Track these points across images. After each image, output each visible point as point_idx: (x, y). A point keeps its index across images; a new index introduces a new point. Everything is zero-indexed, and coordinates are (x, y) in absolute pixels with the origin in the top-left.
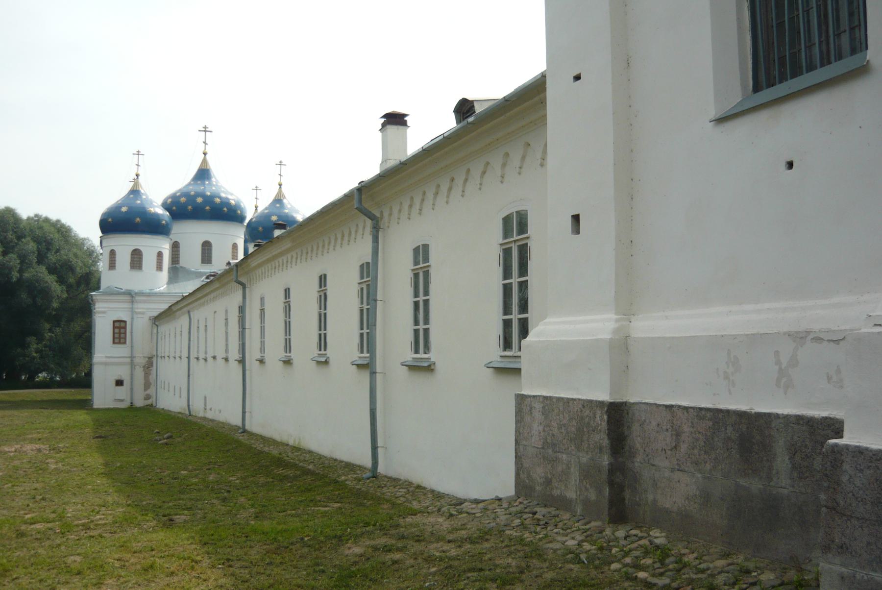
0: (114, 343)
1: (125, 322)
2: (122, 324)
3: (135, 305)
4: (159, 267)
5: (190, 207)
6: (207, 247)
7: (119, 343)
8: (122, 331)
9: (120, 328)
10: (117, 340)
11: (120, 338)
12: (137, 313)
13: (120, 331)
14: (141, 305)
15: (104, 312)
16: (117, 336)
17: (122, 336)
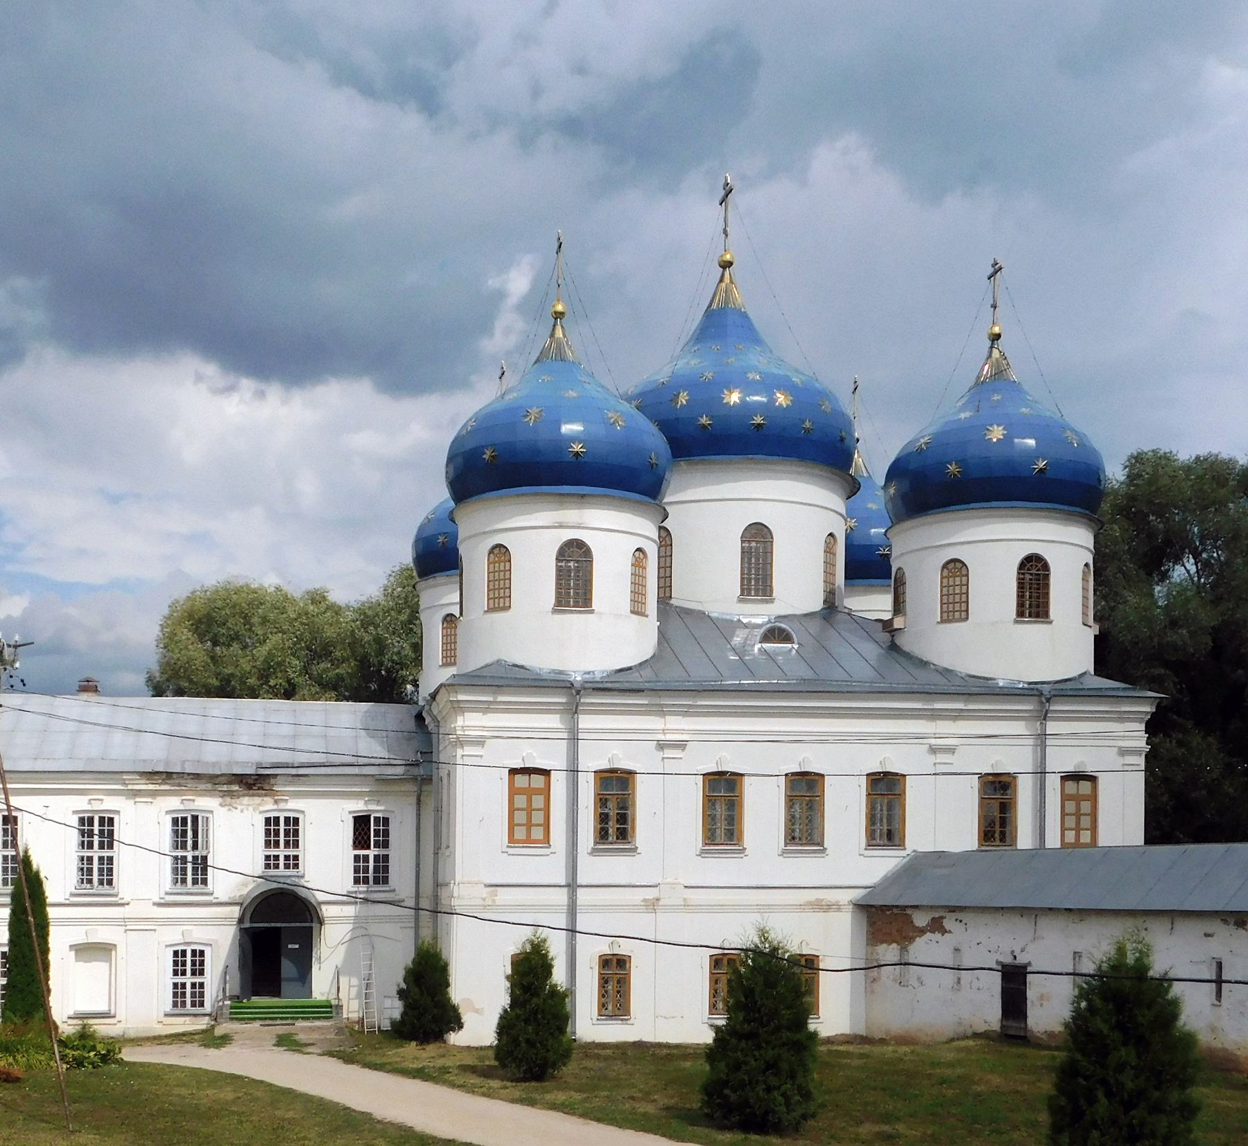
0: (512, 839)
1: (546, 773)
7: (528, 841)
8: (538, 801)
9: (530, 792)
10: (520, 833)
11: (529, 825)
13: (529, 801)
15: (480, 742)
16: (520, 817)
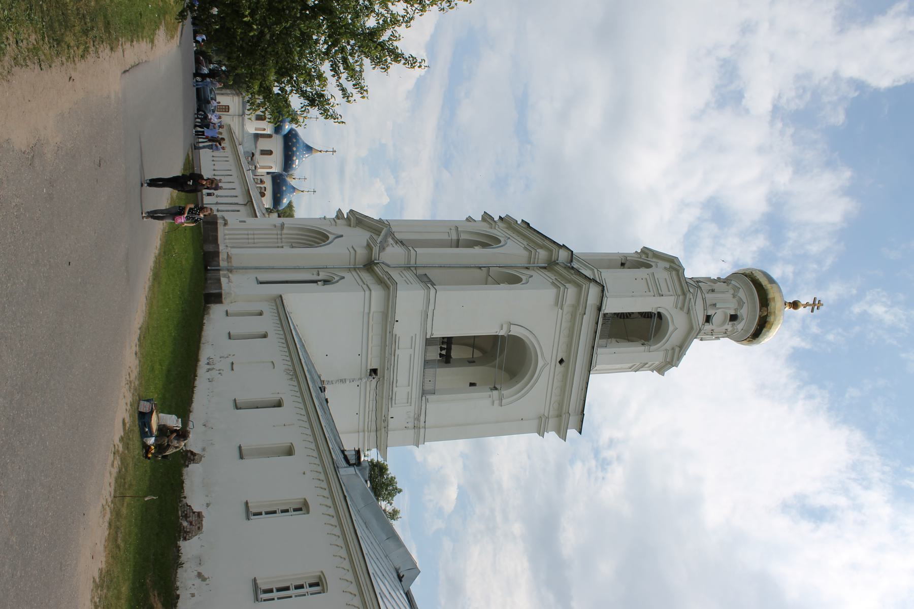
1: (228, 112)
2: (227, 110)
3: (237, 117)
4: (256, 129)
5: (290, 144)
6: (270, 153)
8: (224, 110)
9: (225, 109)
12: (233, 117)
14: (237, 119)
16: (221, 107)
17: (221, 110)
